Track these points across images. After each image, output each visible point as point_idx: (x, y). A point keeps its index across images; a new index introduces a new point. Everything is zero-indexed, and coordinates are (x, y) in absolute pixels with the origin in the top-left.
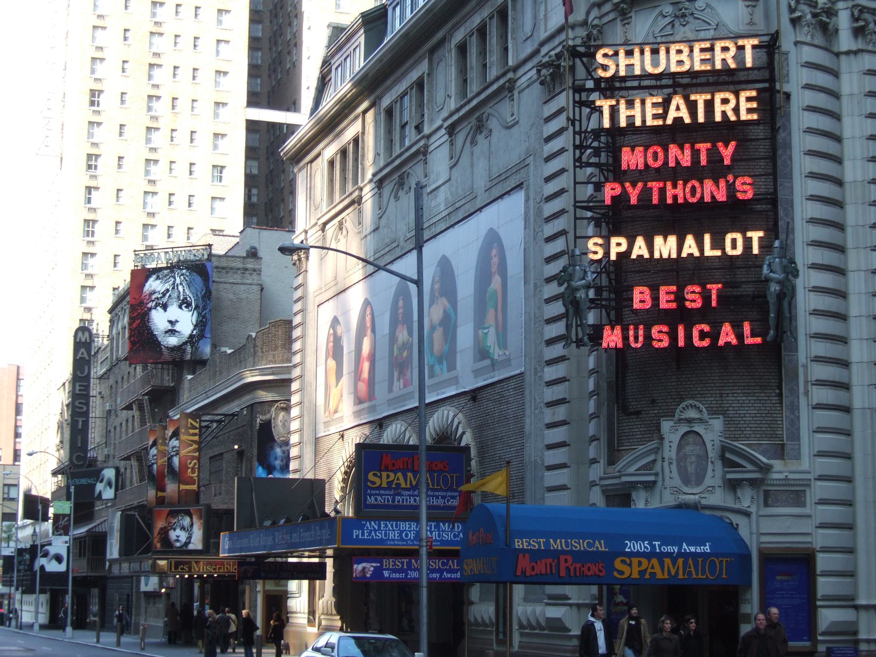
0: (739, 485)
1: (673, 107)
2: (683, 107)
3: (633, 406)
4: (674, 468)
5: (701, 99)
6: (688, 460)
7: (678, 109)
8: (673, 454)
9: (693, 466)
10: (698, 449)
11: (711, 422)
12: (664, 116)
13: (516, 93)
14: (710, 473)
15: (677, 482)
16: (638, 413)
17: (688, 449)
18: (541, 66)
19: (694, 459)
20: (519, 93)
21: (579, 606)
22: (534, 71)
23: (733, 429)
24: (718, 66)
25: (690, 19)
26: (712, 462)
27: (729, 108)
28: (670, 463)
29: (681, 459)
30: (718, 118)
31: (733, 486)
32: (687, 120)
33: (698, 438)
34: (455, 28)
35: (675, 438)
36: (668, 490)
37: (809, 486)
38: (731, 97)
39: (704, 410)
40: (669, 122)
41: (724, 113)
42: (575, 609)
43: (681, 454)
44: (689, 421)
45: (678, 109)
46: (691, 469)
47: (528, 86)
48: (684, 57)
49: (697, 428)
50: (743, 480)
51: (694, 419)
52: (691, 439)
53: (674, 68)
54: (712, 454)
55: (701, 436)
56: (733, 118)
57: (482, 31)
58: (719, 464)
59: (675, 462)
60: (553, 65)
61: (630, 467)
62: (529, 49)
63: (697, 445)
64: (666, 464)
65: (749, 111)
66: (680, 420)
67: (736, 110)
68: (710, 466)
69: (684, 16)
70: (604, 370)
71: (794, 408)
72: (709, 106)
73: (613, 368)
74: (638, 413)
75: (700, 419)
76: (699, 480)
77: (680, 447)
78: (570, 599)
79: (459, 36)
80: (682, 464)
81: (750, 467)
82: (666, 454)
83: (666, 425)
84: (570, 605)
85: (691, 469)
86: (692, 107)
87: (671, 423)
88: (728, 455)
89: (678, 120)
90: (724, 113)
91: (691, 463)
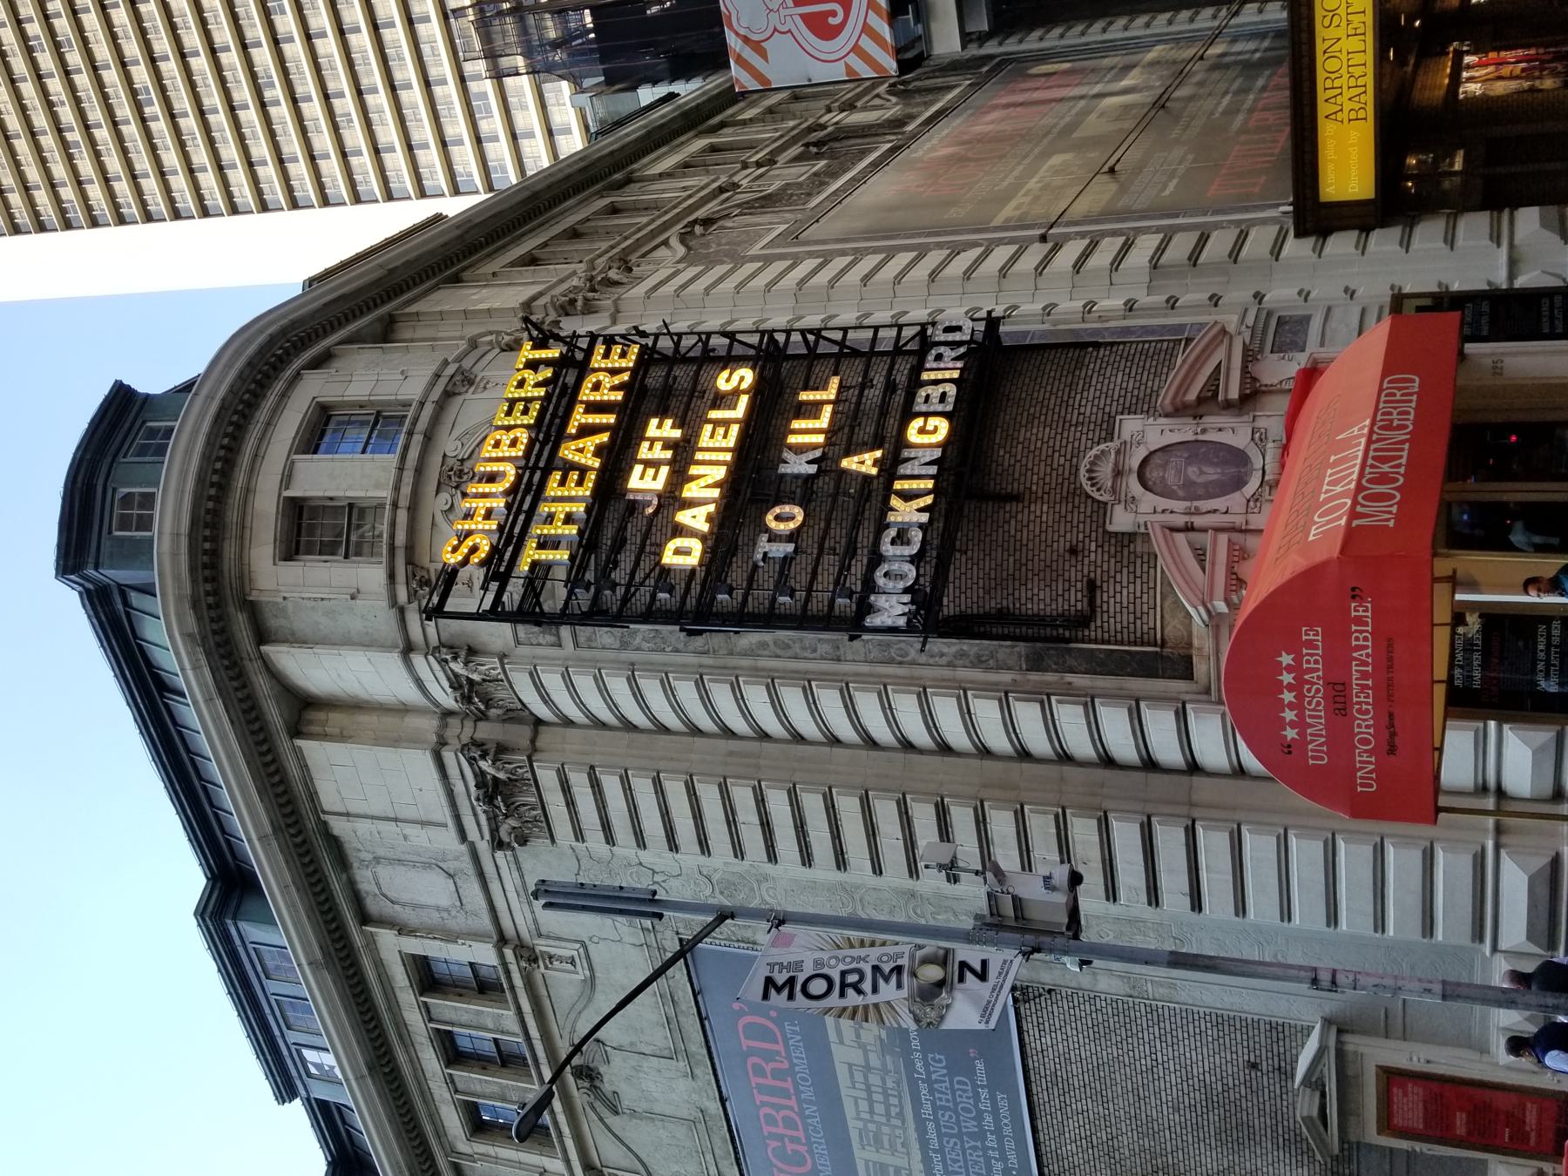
0: (1255, 379)
1: (577, 458)
2: (580, 443)
3: (1076, 600)
4: (1205, 505)
5: (579, 417)
6: (1194, 478)
7: (581, 451)
8: (1179, 505)
9: (1204, 469)
10: (1176, 460)
11: (1126, 436)
12: (583, 470)
13: (542, 946)
14: (1226, 438)
15: (1235, 501)
16: (1092, 587)
17: (1171, 478)
18: (498, 844)
19: (1192, 472)
20: (540, 935)
21: (1499, 830)
22: (499, 854)
23: (1142, 405)
24: (541, 392)
25: (468, 464)
26: (1204, 431)
27: (607, 381)
28: (1197, 512)
29: (1191, 491)
30: (618, 396)
31: (1252, 396)
32: (605, 437)
33: (1157, 460)
34: (440, 1132)
35: (1148, 501)
36: (1251, 517)
37: (1269, 314)
38: (592, 378)
39: (1102, 447)
40: (597, 463)
41: (614, 388)
42: (1504, 839)
43: (1181, 493)
44: (1118, 473)
45: (581, 451)
46: (1212, 474)
47: (519, 869)
48: (506, 438)
49: (1135, 463)
50: (1245, 370)
51: (1116, 464)
52: (1153, 474)
53: (519, 451)
54: (1183, 431)
55: (1152, 453)
56: (626, 377)
57: (453, 1053)
58: (1209, 420)
59: (1196, 503)
60: (491, 790)
61: (1194, 607)
62: (472, 890)
63: (1167, 462)
64: (1198, 521)
65: (623, 355)
66: (1114, 490)
67: (614, 372)
68: (1211, 436)
69: (460, 473)
70: (1006, 677)
71: (1127, 331)
72: (593, 408)
73: (1004, 649)
74: (1092, 587)
75: (1118, 452)
76: (1238, 458)
77: (1169, 495)
78: (1483, 849)
79: (453, 1122)
80: (1201, 492)
81: (1219, 355)
82: (1180, 520)
83: (1121, 521)
84: (1497, 847)
85: (1212, 474)
86: (586, 431)
87: (1119, 509)
88: (1192, 396)
89: (599, 451)
90: (614, 388)
91: (1202, 473)
